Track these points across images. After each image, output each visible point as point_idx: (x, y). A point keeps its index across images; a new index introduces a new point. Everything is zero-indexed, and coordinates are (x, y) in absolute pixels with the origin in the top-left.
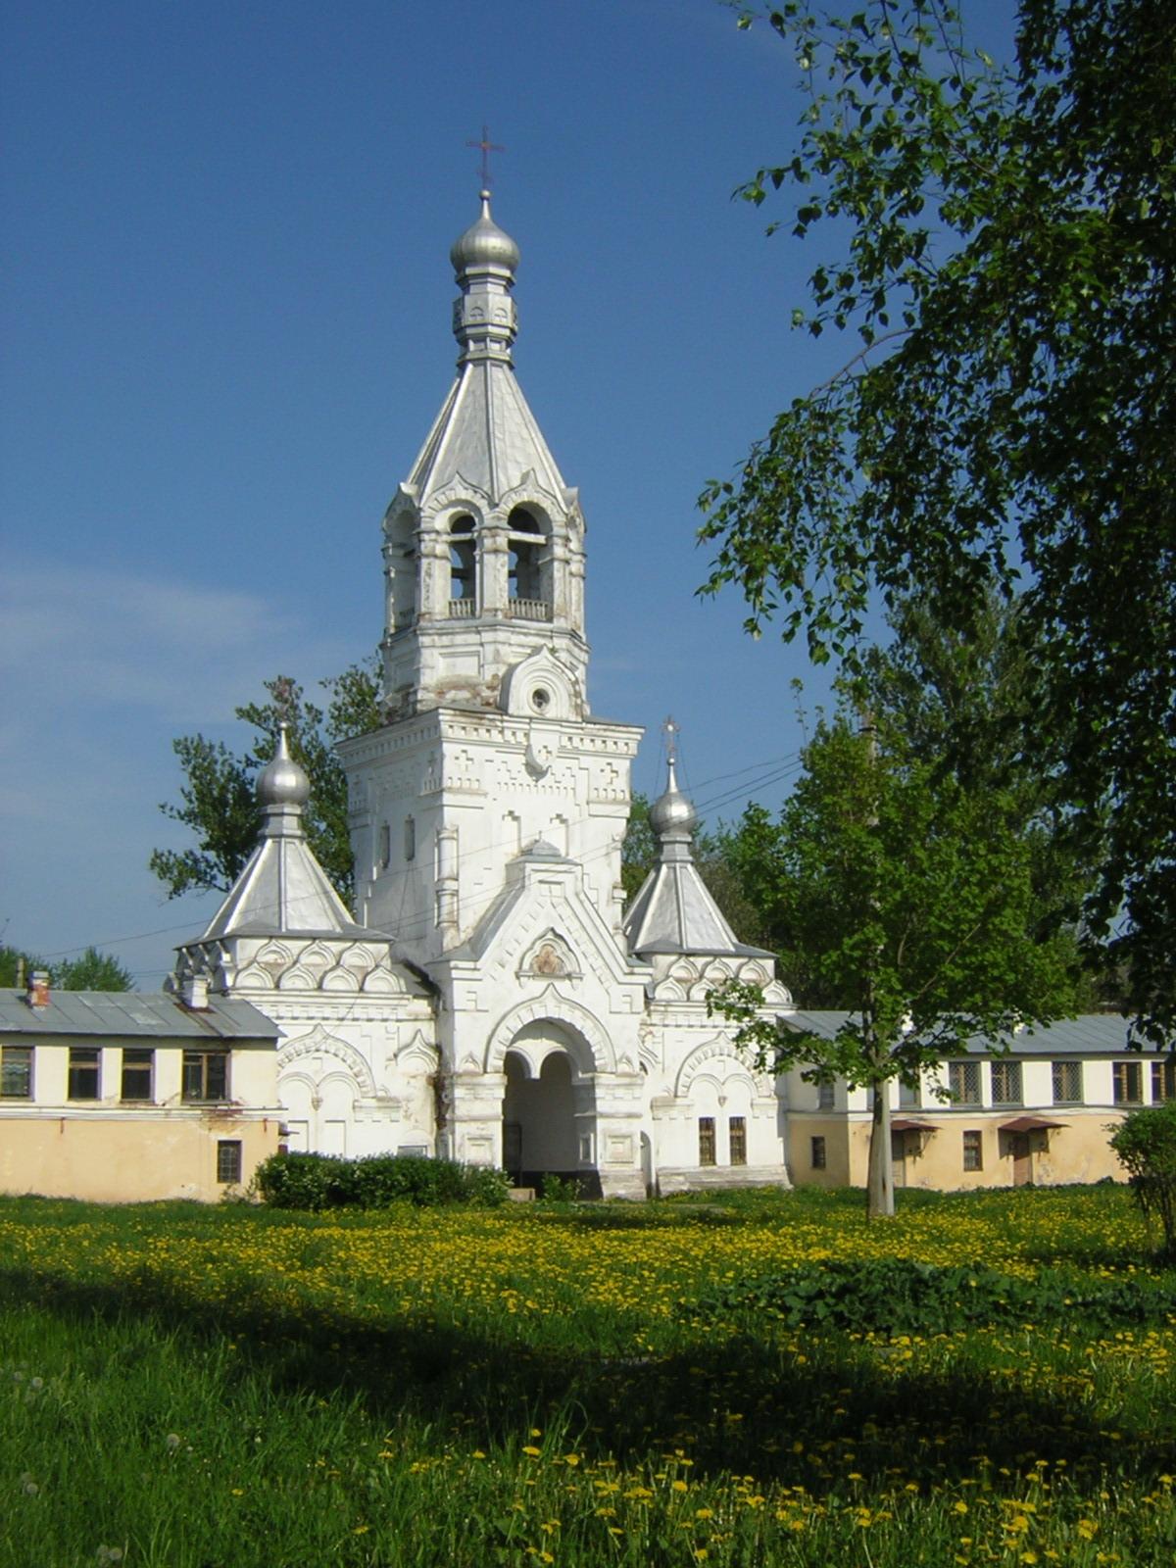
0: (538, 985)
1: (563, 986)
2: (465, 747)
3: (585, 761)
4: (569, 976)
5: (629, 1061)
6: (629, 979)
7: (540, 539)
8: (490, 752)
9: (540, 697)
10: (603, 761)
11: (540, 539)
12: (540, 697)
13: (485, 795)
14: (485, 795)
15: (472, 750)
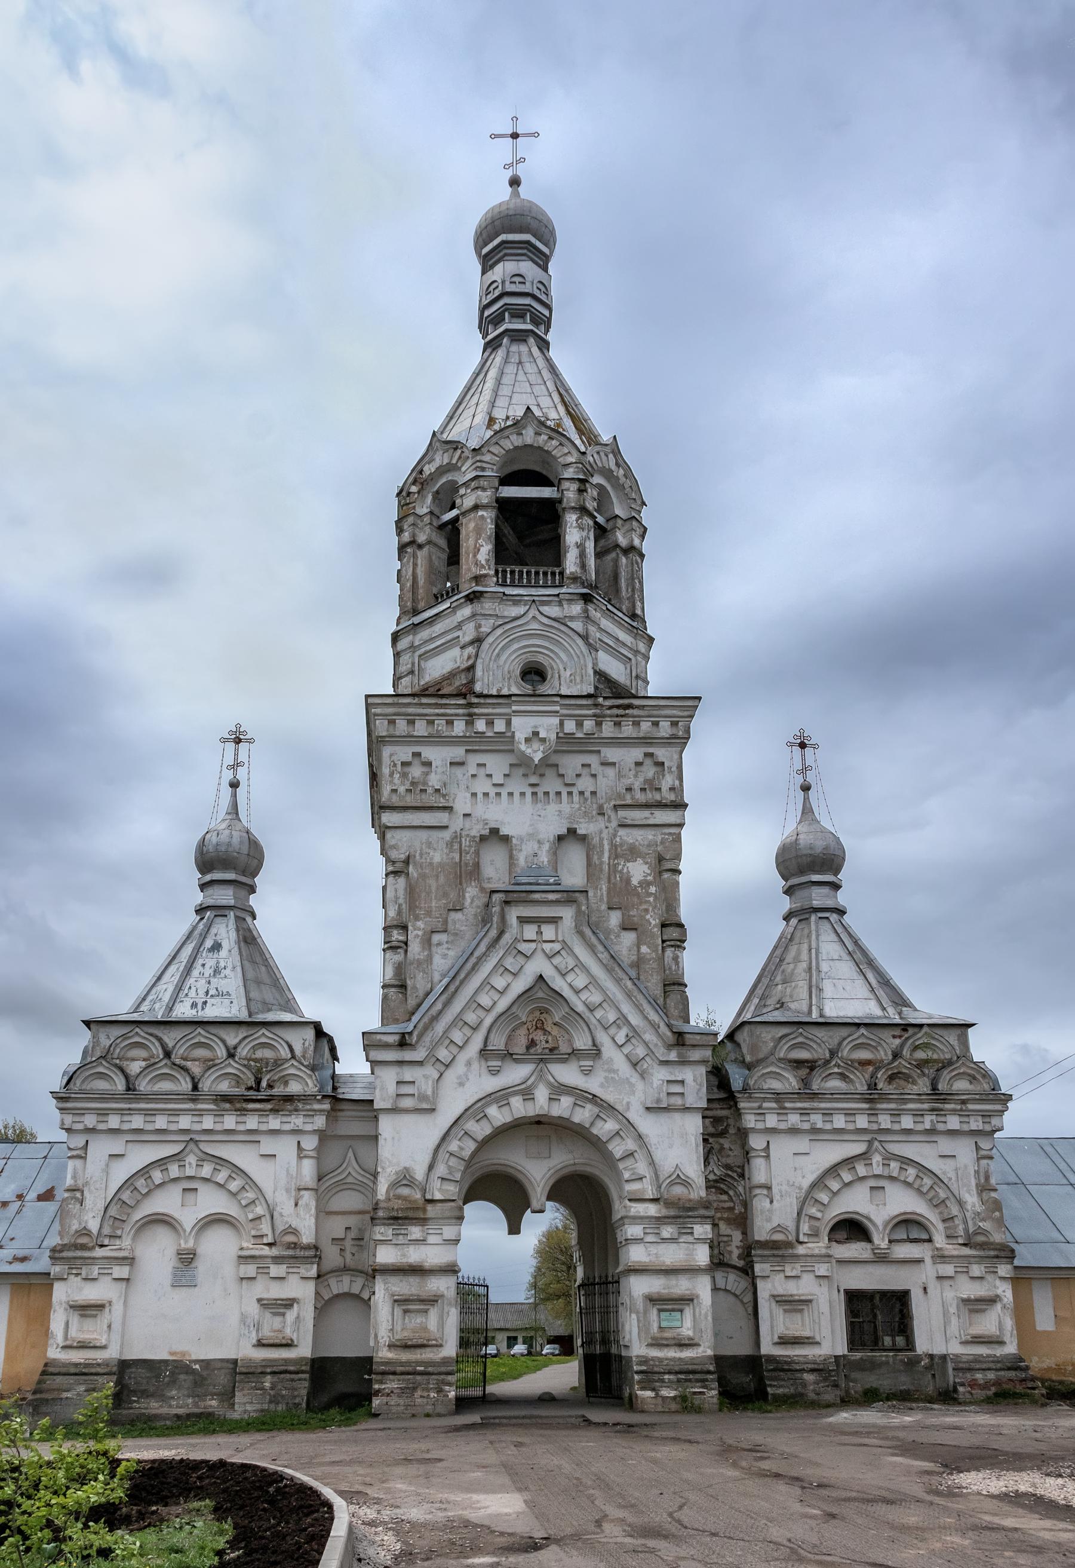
0: (516, 1074)
1: (567, 1074)
2: (417, 749)
3: (611, 754)
4: (575, 1054)
5: (686, 1183)
6: (673, 1056)
7: (546, 492)
8: (458, 752)
9: (534, 673)
10: (637, 753)
11: (546, 492)
12: (534, 673)
13: (449, 809)
14: (449, 809)
15: (428, 752)
